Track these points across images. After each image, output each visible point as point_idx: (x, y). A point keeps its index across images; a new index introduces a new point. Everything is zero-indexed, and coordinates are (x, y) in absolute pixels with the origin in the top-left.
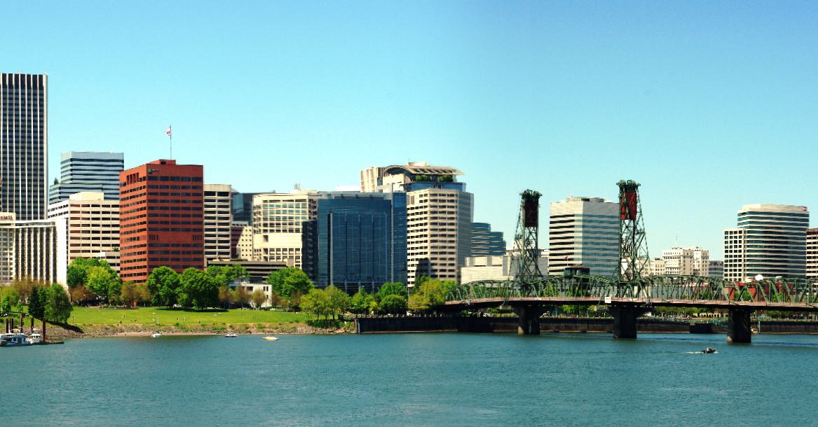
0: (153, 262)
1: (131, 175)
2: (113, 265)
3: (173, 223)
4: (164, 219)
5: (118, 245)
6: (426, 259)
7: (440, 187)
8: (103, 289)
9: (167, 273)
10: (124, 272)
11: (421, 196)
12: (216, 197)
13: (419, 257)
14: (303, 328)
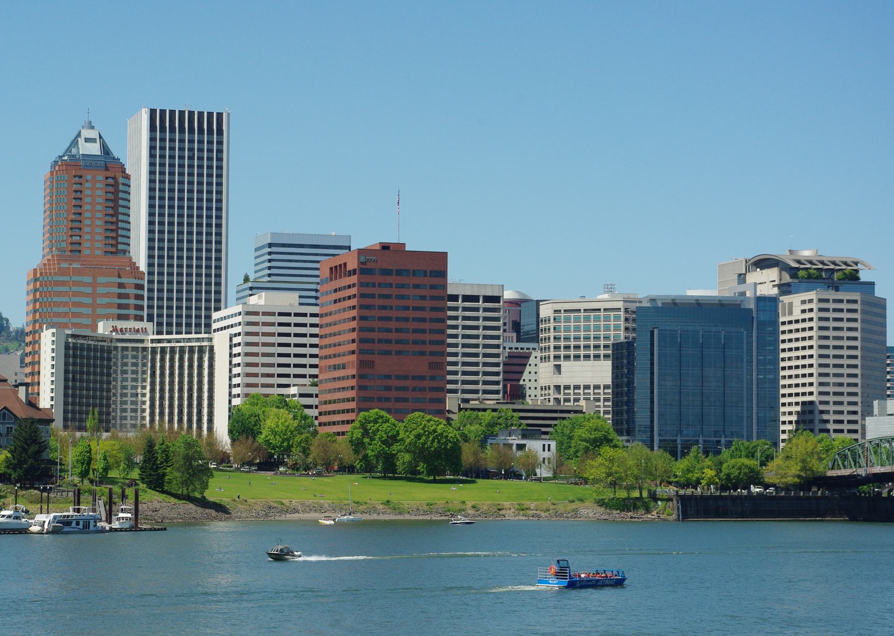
0: (364, 403)
1: (336, 267)
2: (310, 407)
3: (398, 342)
4: (384, 336)
5: (316, 376)
6: (811, 403)
7: (837, 289)
8: (285, 444)
9: (380, 421)
10: (324, 419)
11: (803, 302)
12: (481, 304)
13: (800, 399)
14: (589, 511)
